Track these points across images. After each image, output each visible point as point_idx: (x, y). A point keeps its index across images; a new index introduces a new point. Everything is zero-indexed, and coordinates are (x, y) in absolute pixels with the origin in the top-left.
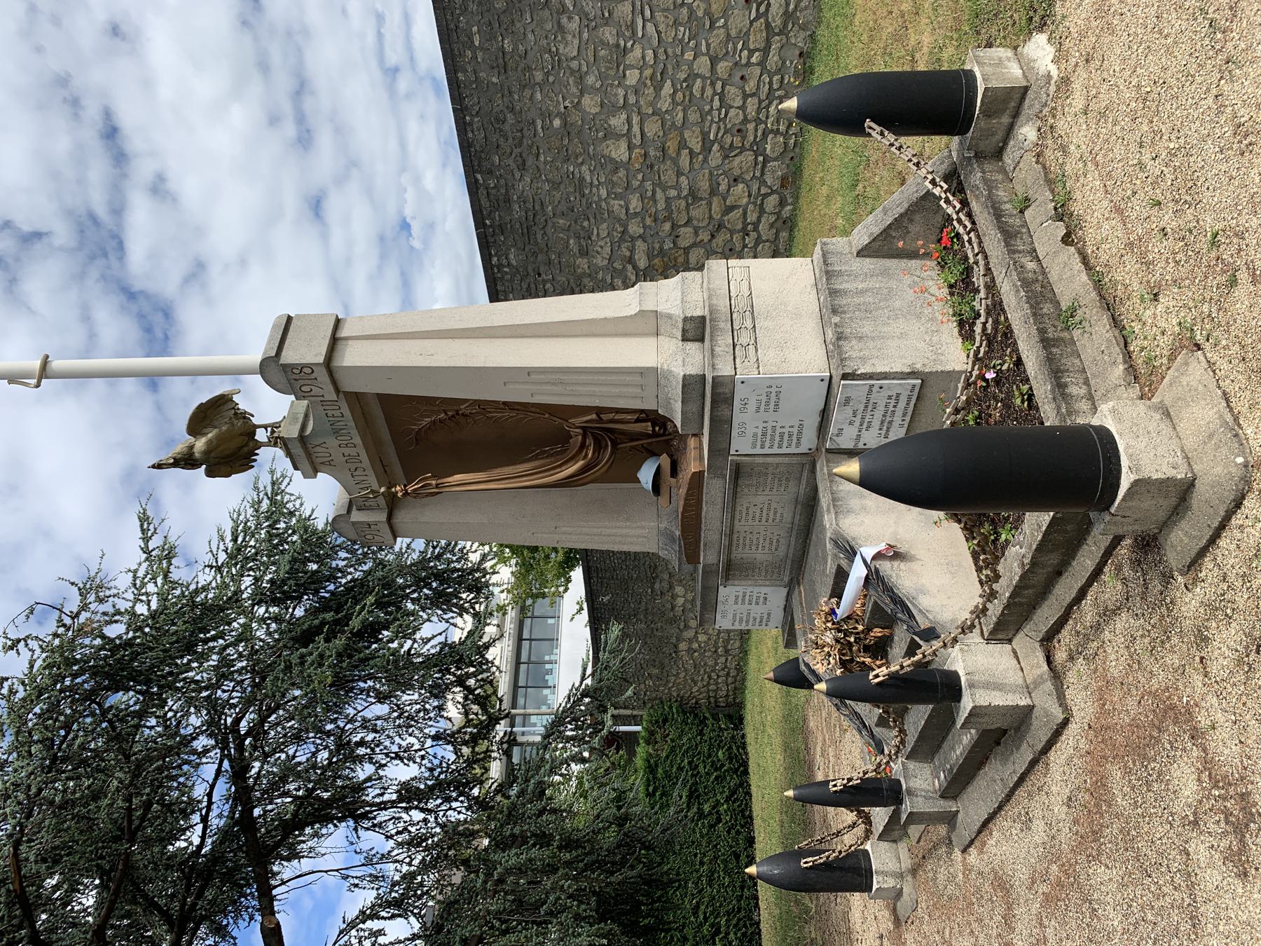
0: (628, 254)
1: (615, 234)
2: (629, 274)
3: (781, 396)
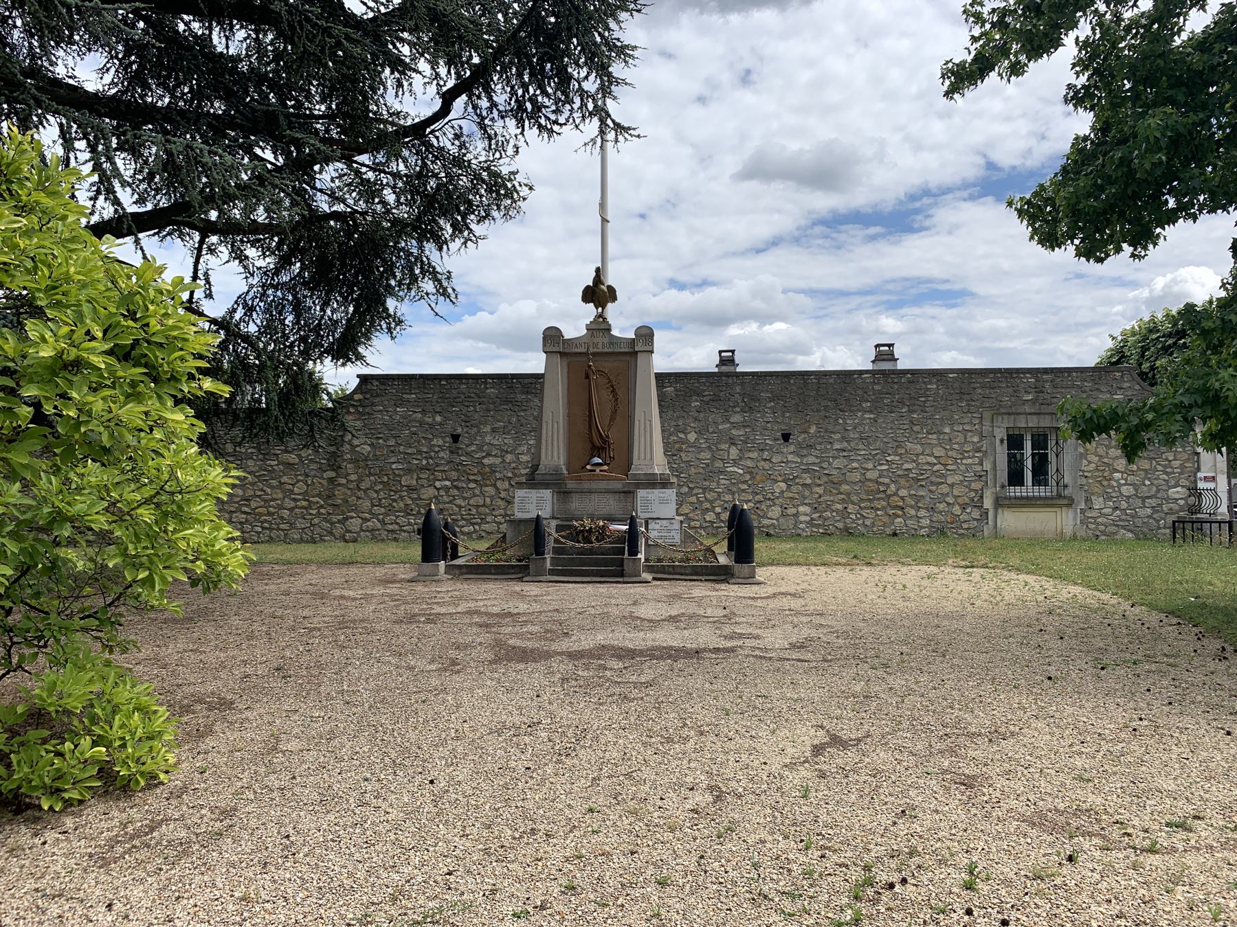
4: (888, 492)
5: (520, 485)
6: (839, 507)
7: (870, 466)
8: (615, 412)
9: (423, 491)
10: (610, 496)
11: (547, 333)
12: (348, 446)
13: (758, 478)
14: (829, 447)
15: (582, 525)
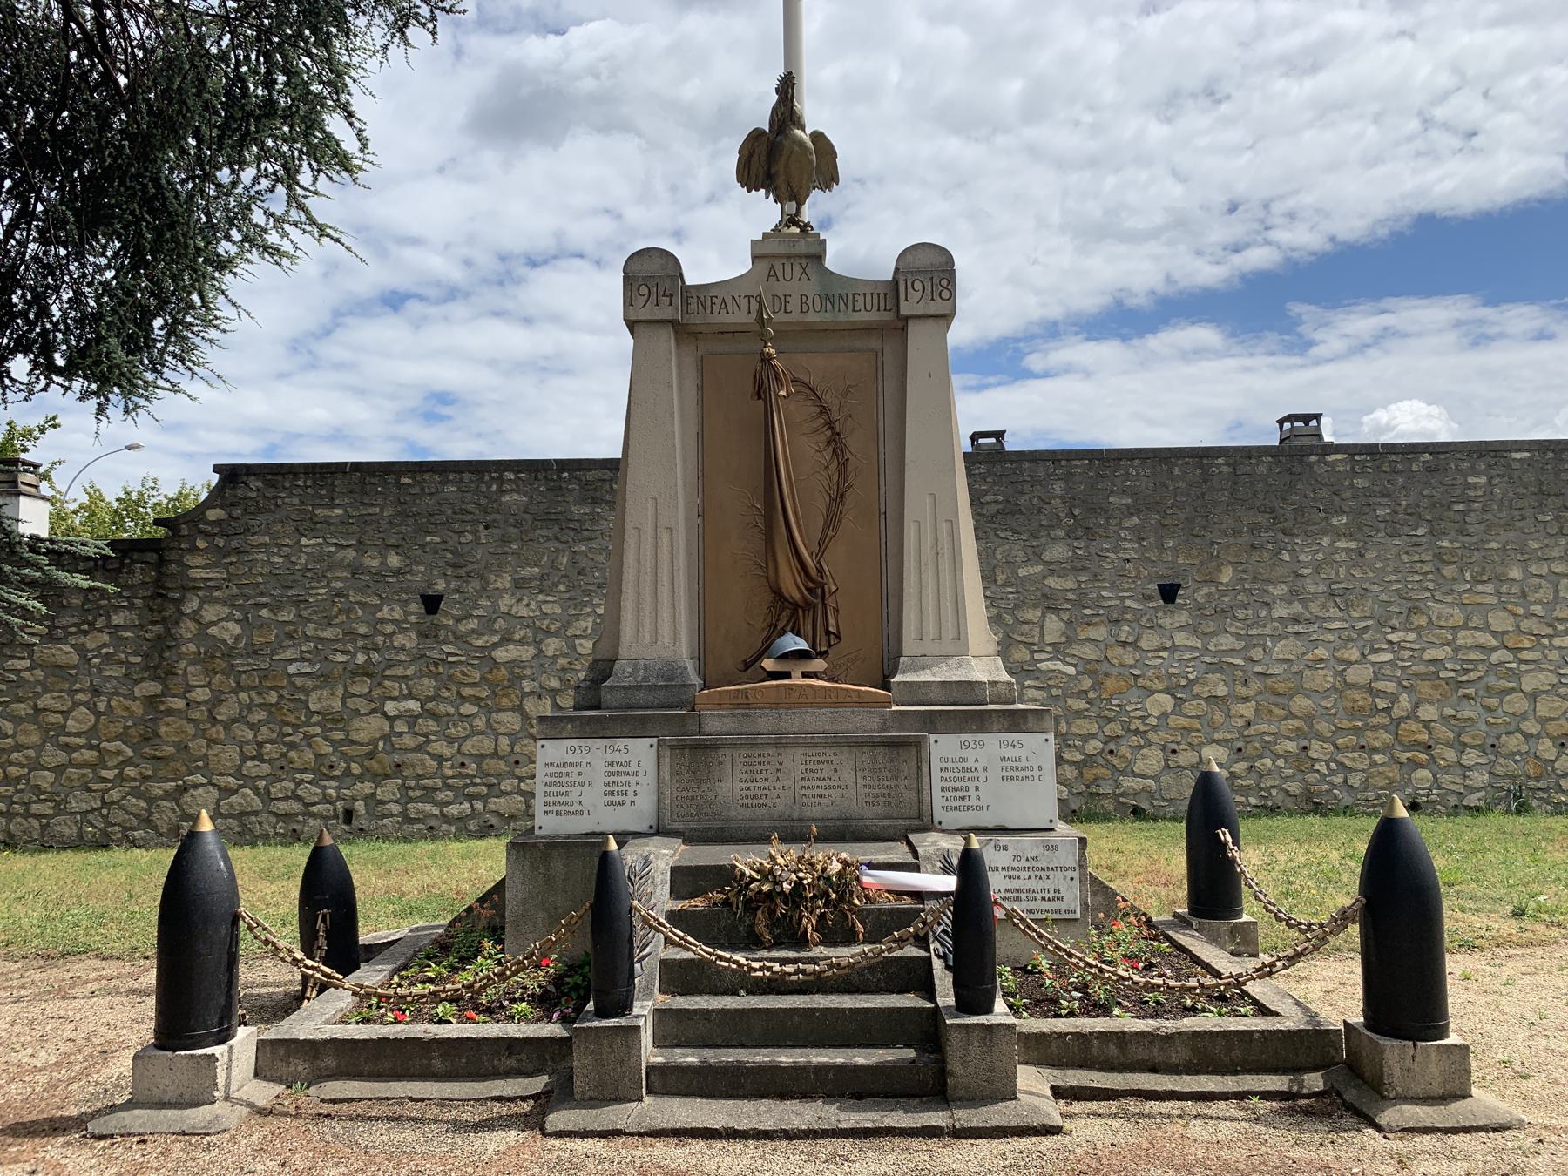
0: (517, 637)
1: (546, 622)
2: (485, 638)
3: (1028, 782)
4: (1396, 713)
5: (553, 727)
6: (1292, 746)
7: (1353, 654)
8: (838, 498)
9: (357, 723)
10: (845, 754)
11: (634, 267)
12: (192, 626)
13: (1110, 684)
14: (1263, 613)
15: (766, 874)
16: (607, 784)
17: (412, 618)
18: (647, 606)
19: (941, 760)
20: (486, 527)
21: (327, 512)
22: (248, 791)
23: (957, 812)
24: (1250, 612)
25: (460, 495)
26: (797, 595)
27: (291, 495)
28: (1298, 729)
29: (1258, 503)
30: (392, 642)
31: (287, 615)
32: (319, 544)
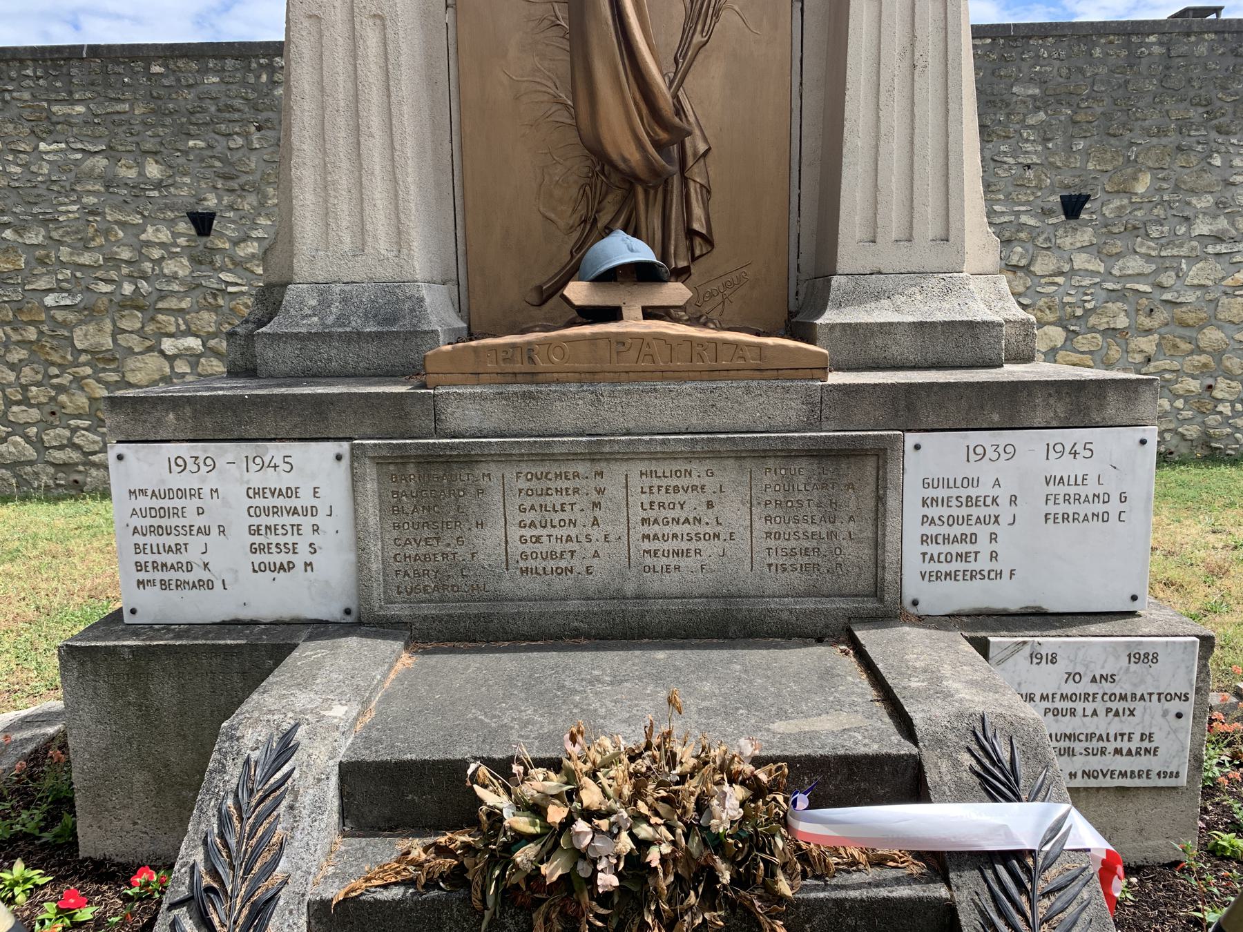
3: (1097, 524)
6: (1194, 385)
9: (131, 363)
10: (729, 474)
14: (1182, 230)
16: (255, 531)
17: (182, 241)
18: (343, 179)
19: (926, 484)
20: (259, 129)
21: (66, 109)
22: (18, 439)
23: (949, 583)
24: (1166, 229)
25: (223, 87)
26: (634, 156)
27: (20, 88)
28: (1205, 365)
29: (1192, 94)
30: (161, 270)
31: (35, 237)
32: (62, 150)
